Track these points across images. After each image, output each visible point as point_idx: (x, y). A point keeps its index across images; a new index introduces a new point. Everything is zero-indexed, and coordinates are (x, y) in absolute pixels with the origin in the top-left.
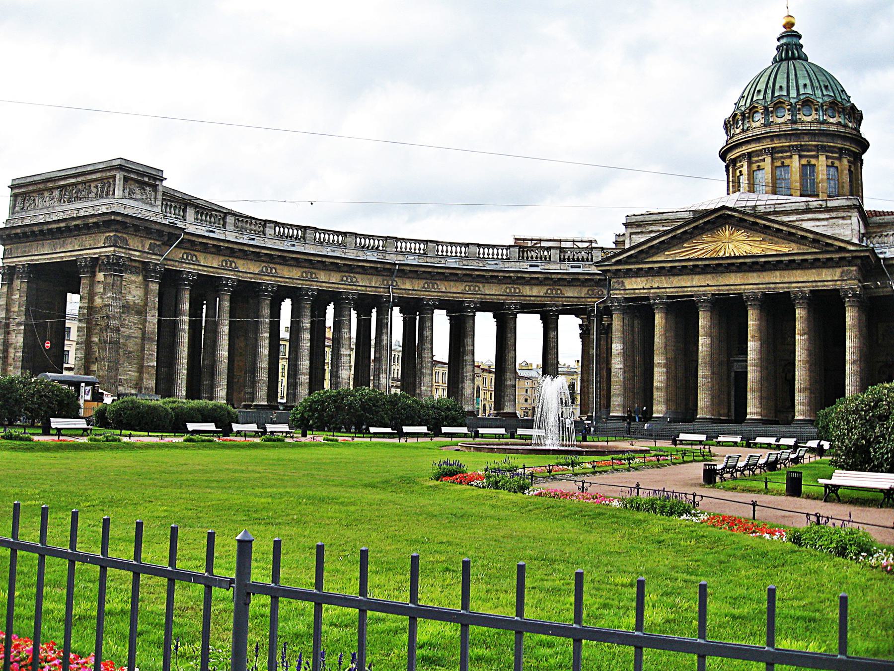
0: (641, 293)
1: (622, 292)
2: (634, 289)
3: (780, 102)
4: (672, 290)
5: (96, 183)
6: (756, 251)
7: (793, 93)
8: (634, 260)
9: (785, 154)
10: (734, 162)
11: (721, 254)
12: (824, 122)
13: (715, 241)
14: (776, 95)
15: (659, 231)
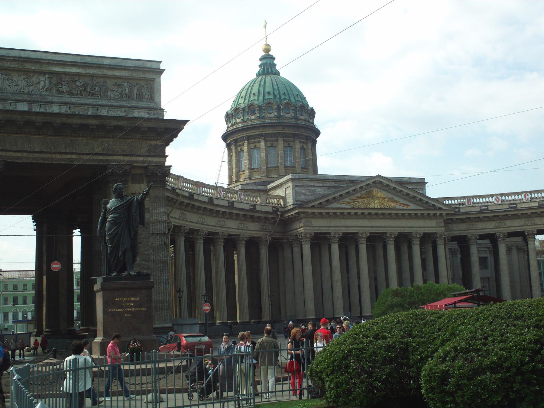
0: (324, 230)
1: (311, 228)
2: (319, 227)
3: (288, 104)
4: (344, 229)
5: (119, 81)
6: (393, 205)
7: (293, 100)
8: (320, 206)
9: (290, 139)
10: (248, 138)
11: (372, 206)
12: (309, 122)
13: (368, 198)
14: (283, 97)
15: (315, 186)
